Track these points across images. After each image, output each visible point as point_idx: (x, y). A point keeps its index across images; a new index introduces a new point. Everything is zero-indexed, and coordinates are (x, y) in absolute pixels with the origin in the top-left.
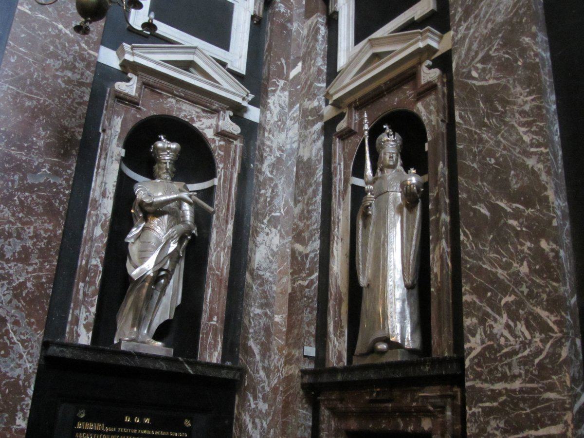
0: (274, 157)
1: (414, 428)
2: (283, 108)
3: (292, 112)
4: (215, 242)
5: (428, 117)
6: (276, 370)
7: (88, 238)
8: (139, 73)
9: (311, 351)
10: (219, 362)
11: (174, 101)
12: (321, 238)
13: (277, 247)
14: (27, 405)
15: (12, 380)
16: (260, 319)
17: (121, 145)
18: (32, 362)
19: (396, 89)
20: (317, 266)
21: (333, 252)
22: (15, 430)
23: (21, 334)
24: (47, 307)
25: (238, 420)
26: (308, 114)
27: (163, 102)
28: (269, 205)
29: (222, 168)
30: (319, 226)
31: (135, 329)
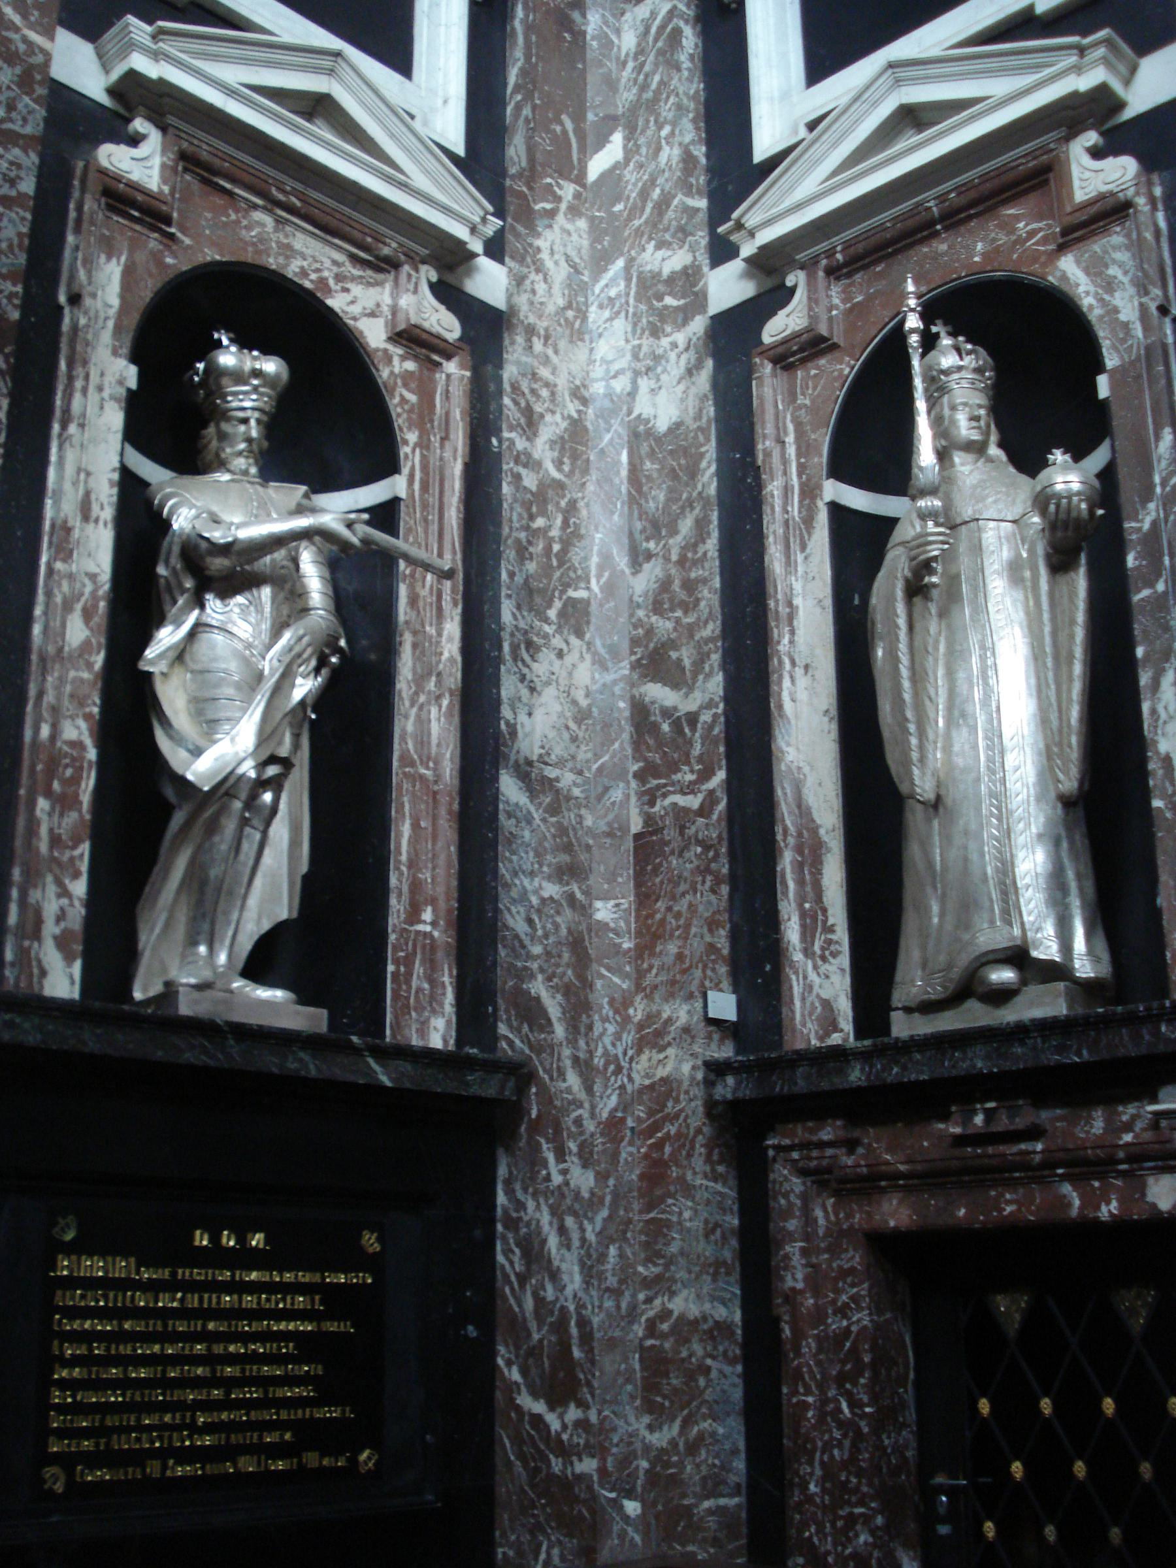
1: (1120, 1208)
2: (574, 267)
3: (603, 283)
4: (410, 677)
5: (1101, 300)
6: (612, 1067)
7: (51, 649)
8: (171, 120)
9: (724, 1005)
10: (451, 1046)
11: (268, 220)
12: (724, 666)
13: (587, 695)
16: (558, 913)
17: (125, 351)
19: (977, 215)
20: (722, 749)
21: (780, 707)
25: (512, 1224)
26: (661, 288)
27: (238, 222)
28: (559, 567)
29: (416, 445)
30: (718, 632)
31: (202, 949)
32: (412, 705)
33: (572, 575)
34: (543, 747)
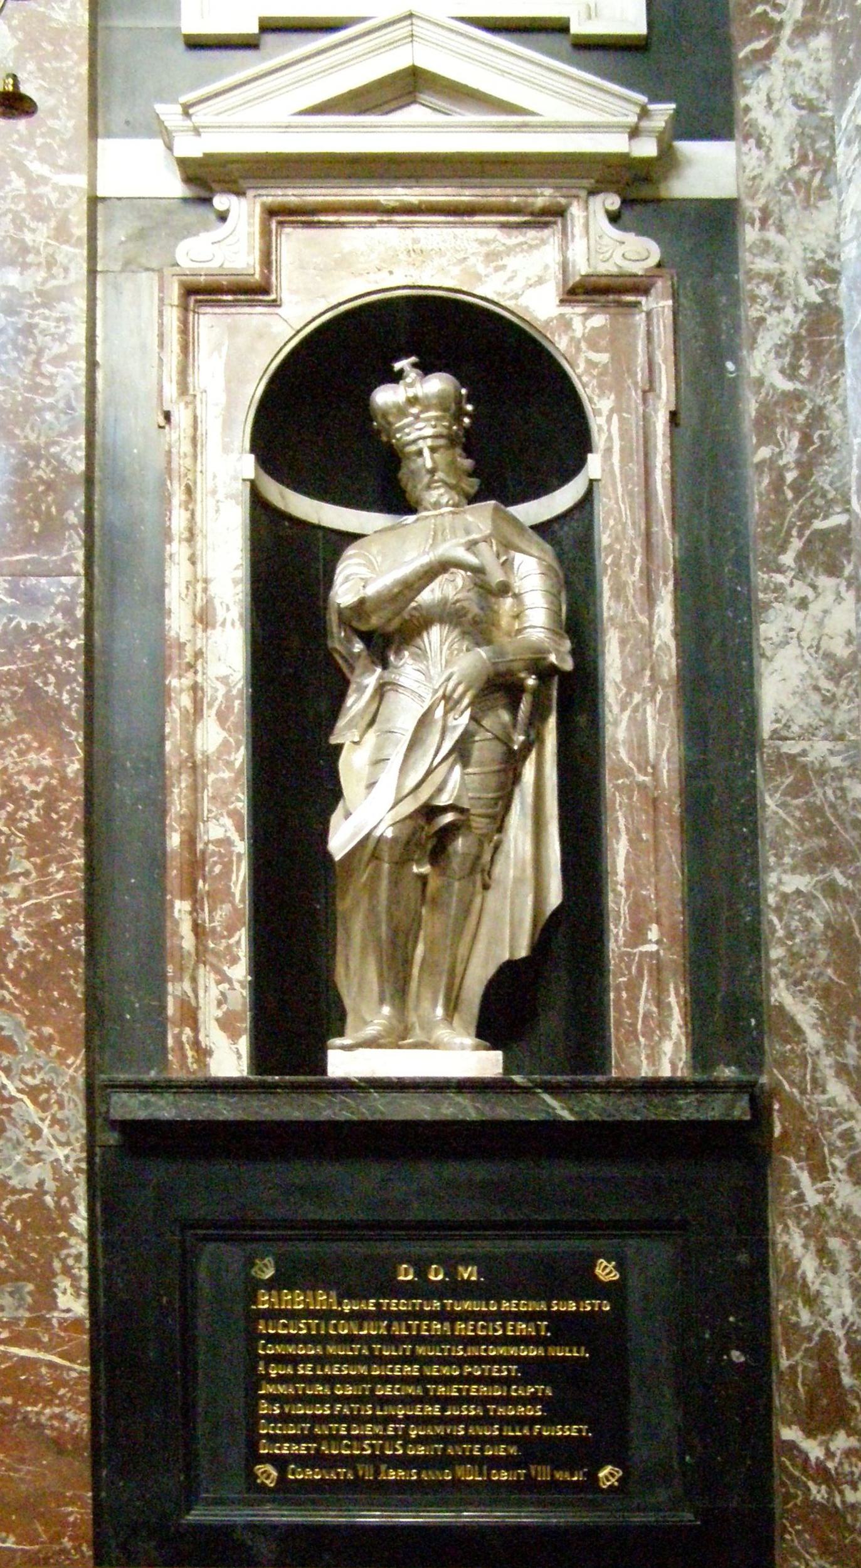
0: (796, 309)
4: (618, 678)
13: (849, 642)
14: (78, 1257)
15: (25, 1196)
16: (809, 906)
18: (68, 1143)
22: (60, 1323)
23: (24, 1072)
24: (79, 990)
28: (796, 498)
32: (623, 709)
33: (818, 501)
34: (778, 721)
